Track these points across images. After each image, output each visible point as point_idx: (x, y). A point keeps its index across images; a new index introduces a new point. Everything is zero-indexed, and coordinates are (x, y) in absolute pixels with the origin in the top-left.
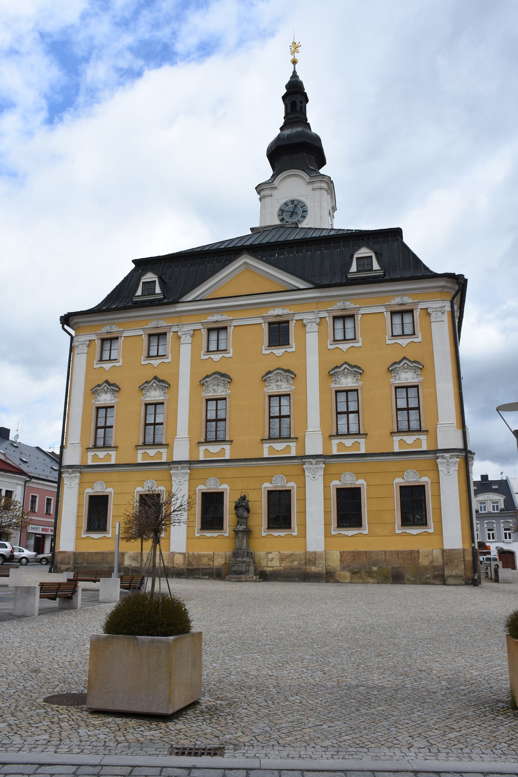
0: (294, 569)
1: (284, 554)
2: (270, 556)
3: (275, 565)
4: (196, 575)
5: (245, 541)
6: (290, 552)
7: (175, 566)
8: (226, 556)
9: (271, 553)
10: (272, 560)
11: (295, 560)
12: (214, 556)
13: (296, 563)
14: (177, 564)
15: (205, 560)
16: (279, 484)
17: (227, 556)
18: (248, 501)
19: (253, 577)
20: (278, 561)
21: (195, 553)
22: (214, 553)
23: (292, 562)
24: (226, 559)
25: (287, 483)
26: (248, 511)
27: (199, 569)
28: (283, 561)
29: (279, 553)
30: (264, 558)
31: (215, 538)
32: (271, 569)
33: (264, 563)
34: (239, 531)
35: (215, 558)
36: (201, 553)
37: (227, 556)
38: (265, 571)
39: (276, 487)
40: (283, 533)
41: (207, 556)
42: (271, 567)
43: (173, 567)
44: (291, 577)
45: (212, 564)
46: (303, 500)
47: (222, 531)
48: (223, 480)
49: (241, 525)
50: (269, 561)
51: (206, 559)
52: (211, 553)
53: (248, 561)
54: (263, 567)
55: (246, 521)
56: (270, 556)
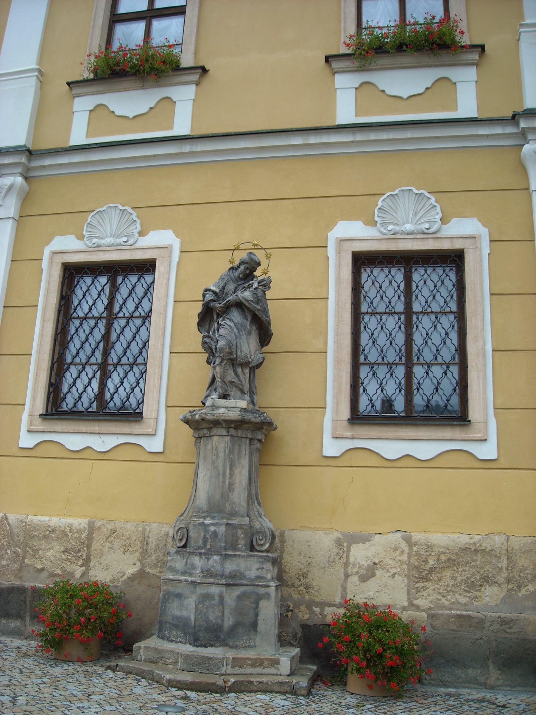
0: (480, 623)
1: (429, 547)
2: (360, 554)
5: (242, 475)
6: (464, 540)
9: (364, 539)
10: (368, 574)
11: (487, 580)
12: (90, 538)
16: (408, 227)
17: (153, 542)
18: (266, 285)
19: (275, 663)
20: (401, 582)
21: (12, 518)
22: (92, 528)
23: (472, 586)
24: (145, 553)
25: (444, 220)
26: (265, 335)
27: (21, 590)
28: (425, 579)
29: (408, 540)
30: (331, 563)
31: (104, 456)
35: (95, 545)
37: (153, 542)
39: (394, 236)
40: (426, 445)
41: (63, 535)
45: (79, 571)
47: (136, 428)
48: (152, 214)
49: (224, 397)
50: (355, 579)
51: (58, 547)
52: (79, 522)
53: (252, 573)
54: (323, 605)
55: (252, 380)
56: (360, 554)
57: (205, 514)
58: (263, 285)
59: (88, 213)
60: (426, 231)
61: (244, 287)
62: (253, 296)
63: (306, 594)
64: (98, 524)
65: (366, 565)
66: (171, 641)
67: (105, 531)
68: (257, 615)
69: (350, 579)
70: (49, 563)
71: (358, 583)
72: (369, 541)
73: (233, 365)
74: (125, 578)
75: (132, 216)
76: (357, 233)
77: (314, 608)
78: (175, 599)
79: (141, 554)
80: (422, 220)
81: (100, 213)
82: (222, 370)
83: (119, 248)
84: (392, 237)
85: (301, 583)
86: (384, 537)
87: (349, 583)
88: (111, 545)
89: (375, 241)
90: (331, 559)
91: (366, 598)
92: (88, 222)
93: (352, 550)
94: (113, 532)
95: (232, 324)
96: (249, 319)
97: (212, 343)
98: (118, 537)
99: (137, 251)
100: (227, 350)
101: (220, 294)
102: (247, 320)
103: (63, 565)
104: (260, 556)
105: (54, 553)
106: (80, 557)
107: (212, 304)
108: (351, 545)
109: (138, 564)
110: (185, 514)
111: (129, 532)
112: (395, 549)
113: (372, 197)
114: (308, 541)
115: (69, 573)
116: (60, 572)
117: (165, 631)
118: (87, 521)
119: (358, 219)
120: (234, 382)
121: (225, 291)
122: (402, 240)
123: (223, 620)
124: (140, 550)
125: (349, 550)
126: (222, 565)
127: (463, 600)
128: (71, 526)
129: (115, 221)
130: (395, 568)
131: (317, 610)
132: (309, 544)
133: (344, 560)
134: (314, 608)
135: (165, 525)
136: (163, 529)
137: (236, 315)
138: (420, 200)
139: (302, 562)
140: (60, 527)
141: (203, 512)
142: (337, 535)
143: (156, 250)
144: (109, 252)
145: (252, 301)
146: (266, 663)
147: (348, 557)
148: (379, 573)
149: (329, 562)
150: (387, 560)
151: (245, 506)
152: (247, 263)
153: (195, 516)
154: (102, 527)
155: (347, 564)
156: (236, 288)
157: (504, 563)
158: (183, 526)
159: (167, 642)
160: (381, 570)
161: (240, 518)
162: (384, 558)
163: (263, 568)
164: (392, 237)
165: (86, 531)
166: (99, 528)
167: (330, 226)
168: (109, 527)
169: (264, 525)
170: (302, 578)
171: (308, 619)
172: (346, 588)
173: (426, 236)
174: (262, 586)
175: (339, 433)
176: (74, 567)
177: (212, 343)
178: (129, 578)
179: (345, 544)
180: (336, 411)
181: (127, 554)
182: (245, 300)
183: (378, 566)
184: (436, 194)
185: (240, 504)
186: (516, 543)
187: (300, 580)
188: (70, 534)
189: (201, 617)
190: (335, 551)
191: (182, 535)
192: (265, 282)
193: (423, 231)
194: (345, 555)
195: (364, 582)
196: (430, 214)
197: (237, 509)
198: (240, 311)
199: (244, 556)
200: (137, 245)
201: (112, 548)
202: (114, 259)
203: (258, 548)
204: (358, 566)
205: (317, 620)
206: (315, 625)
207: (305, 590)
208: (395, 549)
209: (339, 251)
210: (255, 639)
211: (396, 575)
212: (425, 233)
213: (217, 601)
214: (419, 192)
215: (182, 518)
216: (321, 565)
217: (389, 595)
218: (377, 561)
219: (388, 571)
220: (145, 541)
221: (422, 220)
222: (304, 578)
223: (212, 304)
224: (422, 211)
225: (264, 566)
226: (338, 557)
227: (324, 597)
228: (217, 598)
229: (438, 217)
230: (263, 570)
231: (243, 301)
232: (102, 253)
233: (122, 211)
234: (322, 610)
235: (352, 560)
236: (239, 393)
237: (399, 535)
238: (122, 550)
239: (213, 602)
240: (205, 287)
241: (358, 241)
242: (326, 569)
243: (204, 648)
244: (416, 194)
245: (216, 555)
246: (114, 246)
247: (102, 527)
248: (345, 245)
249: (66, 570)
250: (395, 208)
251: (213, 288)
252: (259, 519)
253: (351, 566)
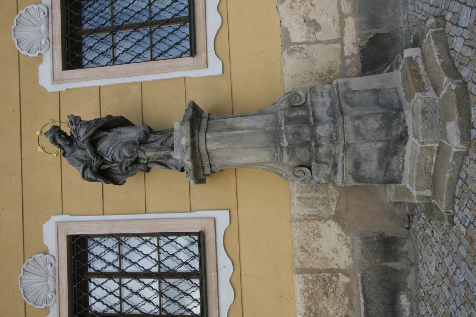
2: (298, 34)
8: (307, 218)
9: (285, 32)
12: (311, 271)
16: (43, 27)
19: (411, 60)
22: (302, 271)
24: (319, 218)
26: (122, 122)
31: (237, 265)
32: (350, 23)
33: (325, 57)
34: (194, 145)
35: (318, 265)
37: (307, 211)
38: (362, 51)
41: (311, 297)
42: (342, 25)
45: (344, 279)
50: (320, 35)
52: (298, 282)
54: (343, 57)
56: (298, 34)
57: (279, 149)
58: (75, 121)
59: (27, 306)
60: (46, 14)
61: (77, 138)
62: (83, 128)
63: (336, 72)
64: (298, 265)
65: (307, 28)
66: (403, 168)
67: (303, 257)
68: (366, 91)
69: (319, 39)
70: (340, 310)
71: (322, 32)
72: (287, 29)
73: (146, 143)
74: (343, 233)
75: (30, 262)
76: (48, 71)
77: (347, 64)
78: (362, 168)
79: (319, 220)
80: (39, 19)
81: (26, 294)
82: (149, 150)
83: (57, 271)
84: (51, 40)
85: (327, 78)
86: (282, 18)
87: (323, 39)
88: (315, 250)
89: (54, 53)
90: (305, 56)
91: (334, 24)
92: (33, 304)
93: (296, 41)
94: (303, 249)
95: (111, 149)
96: (106, 133)
97: (125, 162)
98: (307, 244)
99: (60, 253)
100: (131, 145)
101: (85, 163)
102: (107, 135)
103: (339, 296)
104: (311, 96)
105: (330, 306)
106: (330, 280)
107: (94, 168)
108: (292, 43)
109: (329, 222)
110: (280, 172)
111: (302, 234)
112: (292, 7)
113: (20, 57)
114: (292, 77)
115: (346, 289)
116: (347, 299)
117: (394, 176)
118: (296, 276)
119: (37, 70)
120: (162, 143)
121: (83, 159)
122: (54, 33)
123: (378, 114)
124: (316, 221)
125: (296, 43)
126: (324, 123)
128: (303, 291)
129: (33, 278)
130: (306, 5)
131: (348, 62)
132: (294, 76)
133: (304, 46)
134: (347, 64)
135: (292, 201)
136: (295, 202)
137: (103, 146)
138: (22, 23)
139: (309, 79)
140: (305, 302)
141: (277, 152)
142: (285, 55)
143: (60, 236)
144: (60, 280)
145: (88, 128)
146: (413, 68)
147: (301, 43)
148: (312, 17)
149: (307, 58)
150: (302, 12)
151: (267, 115)
152: (54, 136)
153: (282, 160)
154: (300, 260)
155: (307, 43)
156: (80, 148)
158: (291, 173)
159: (404, 173)
160: (309, 16)
161: (279, 117)
162: (300, 15)
163: (321, 93)
164: (51, 40)
165: (306, 275)
166: (301, 263)
167: (43, 90)
168: (299, 253)
169: (282, 99)
170: (323, 78)
171: (357, 68)
172: (327, 41)
173: (50, 15)
174: (337, 89)
175: (203, 63)
176: (340, 284)
177: (125, 162)
178: (343, 229)
179: (292, 47)
180: (187, 68)
181: (322, 233)
182: (86, 133)
183: (306, 18)
184: (19, 9)
185: (266, 120)
187: (325, 79)
188: (310, 292)
189: (378, 135)
190: (298, 54)
191: (300, 172)
192: (73, 120)
193: (46, 17)
194: (300, 46)
195: (320, 27)
196: (34, 14)
197: (271, 122)
198: (99, 142)
199: (312, 109)
200: (55, 254)
201: (318, 249)
202: (66, 275)
203: (304, 101)
204: (308, 34)
205: (358, 61)
206: (362, 62)
207: (333, 74)
208: (292, 7)
209: (62, 81)
210: (389, 89)
211: (313, 3)
212: (48, 16)
213: (360, 121)
214: (15, 22)
215: (284, 175)
216: (310, 64)
217: (329, 6)
218: (303, 20)
219: (310, 10)
220: (307, 218)
221: (39, 19)
222: (323, 76)
223: (94, 168)
224: (31, 20)
225: (319, 92)
226: (303, 51)
227: (336, 56)
228: (357, 122)
229: (36, 7)
230: (323, 92)
231: (87, 135)
232: (61, 287)
233: (25, 273)
234: (348, 57)
235: (304, 40)
236: (171, 139)
237: (280, 7)
238: (318, 239)
239: (361, 126)
240: (81, 178)
241: (54, 67)
242: (313, 59)
243: (408, 129)
244: (17, 24)
245: (315, 131)
246: (55, 276)
247: (300, 260)
248: (57, 76)
249: (344, 293)
250: (30, 42)
251: (81, 170)
252: (277, 104)
253: (309, 40)
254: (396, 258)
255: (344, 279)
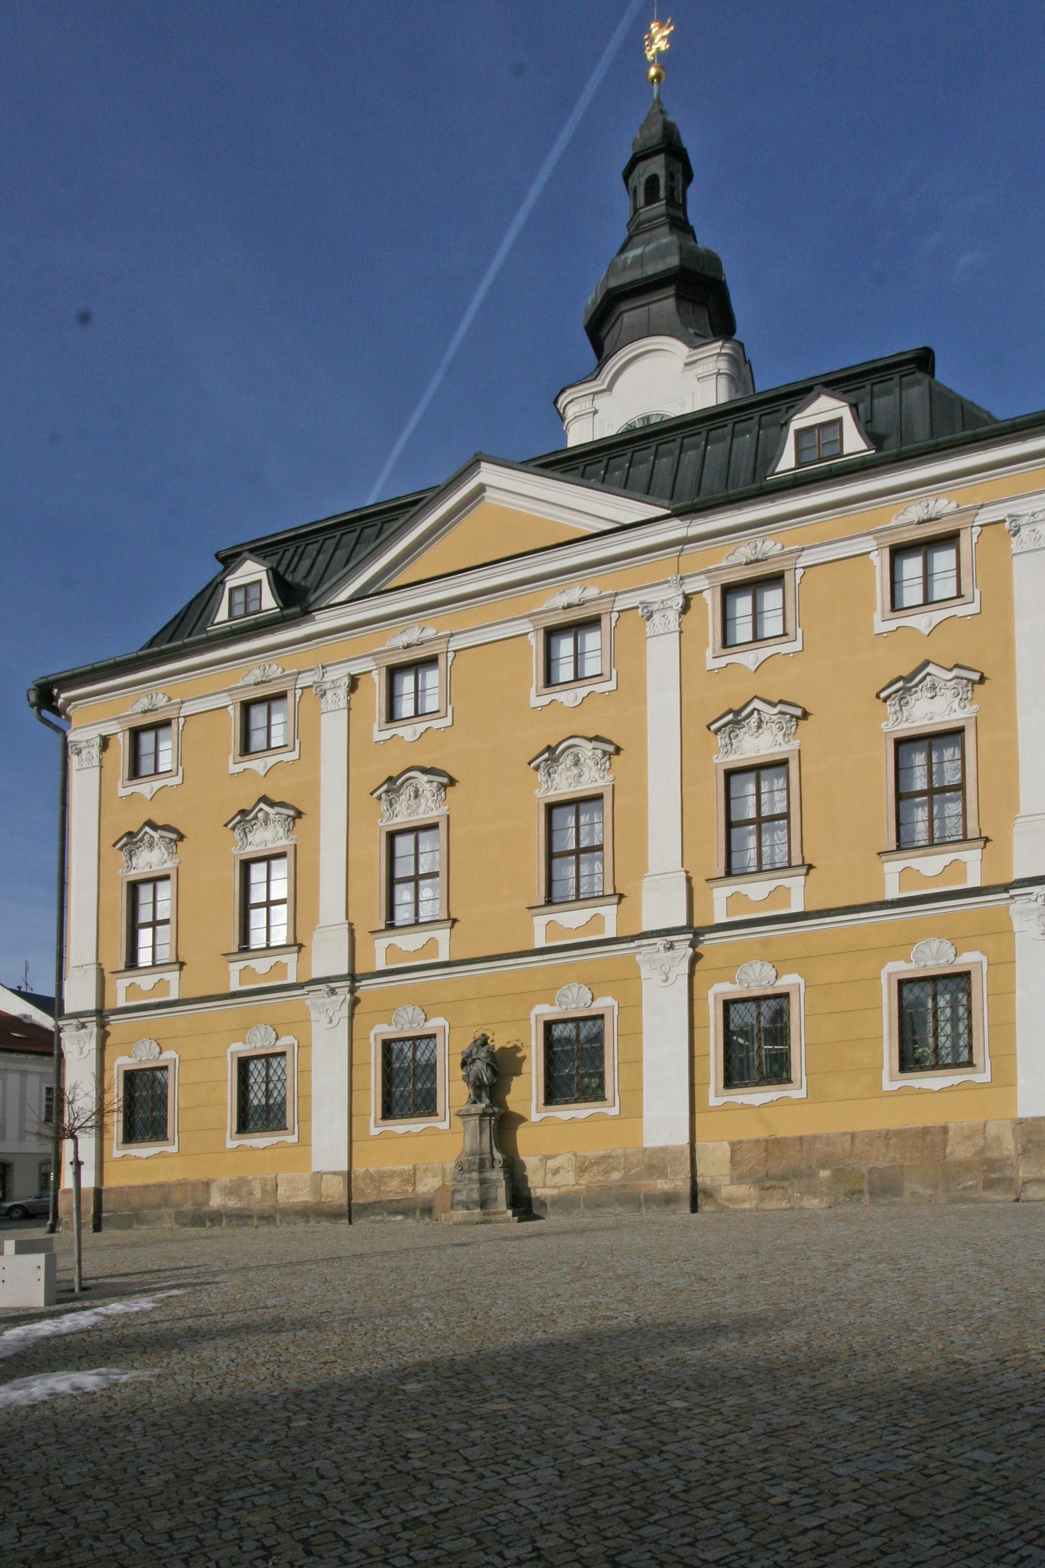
0: (611, 1188)
1: (585, 1157)
3: (564, 1182)
4: (374, 1214)
6: (602, 1153)
7: (323, 1200)
9: (554, 1157)
10: (556, 1172)
11: (614, 1169)
13: (616, 1176)
14: (327, 1196)
15: (394, 1184)
21: (371, 1170)
23: (607, 1172)
24: (443, 1177)
28: (584, 1171)
29: (575, 1154)
32: (555, 1192)
35: (418, 1176)
36: (385, 1168)
37: (448, 1170)
41: (400, 1174)
42: (555, 1187)
43: (320, 1202)
44: (604, 1206)
46: (633, 1034)
50: (549, 1175)
51: (398, 1180)
52: (408, 1167)
56: (552, 1164)
67: (423, 1168)
94: (427, 1169)
127: (602, 1179)
148: (562, 1171)
157: (622, 1160)
186: (629, 1151)
220: (444, 1170)
254: (421, 1214)
255: (410, 1190)
